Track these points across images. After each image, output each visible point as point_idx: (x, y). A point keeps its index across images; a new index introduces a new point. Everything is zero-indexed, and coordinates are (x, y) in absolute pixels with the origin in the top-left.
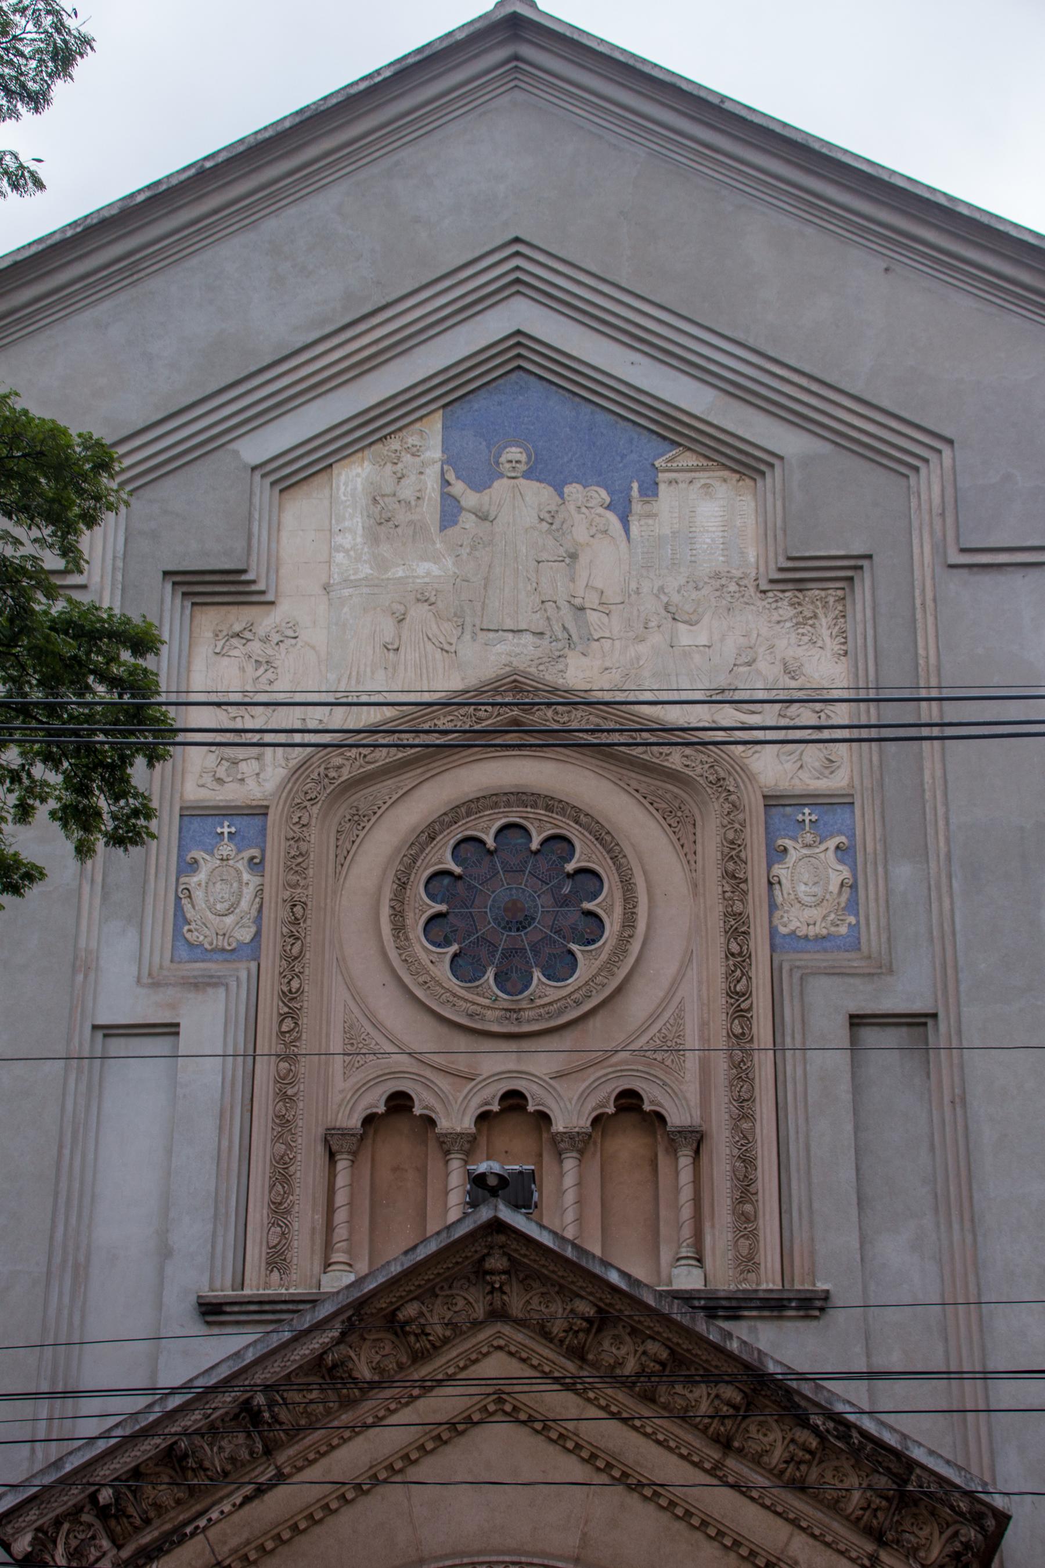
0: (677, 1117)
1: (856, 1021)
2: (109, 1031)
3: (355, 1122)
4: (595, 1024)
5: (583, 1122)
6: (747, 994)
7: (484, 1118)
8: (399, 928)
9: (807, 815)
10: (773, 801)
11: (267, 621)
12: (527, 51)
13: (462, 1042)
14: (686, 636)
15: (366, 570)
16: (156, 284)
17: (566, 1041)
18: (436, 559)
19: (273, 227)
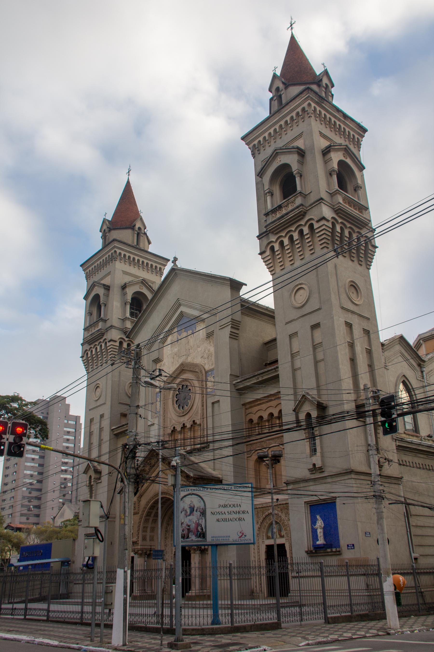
0: (198, 423)
1: (213, 403)
2: (150, 426)
3: (170, 432)
4: (191, 411)
5: (190, 426)
6: (203, 403)
7: (182, 428)
8: (173, 404)
9: (210, 373)
10: (206, 372)
11: (162, 363)
12: (177, 271)
13: (179, 418)
14: (199, 349)
15: (171, 352)
16: (148, 322)
17: (188, 414)
18: (176, 348)
19: (158, 308)
